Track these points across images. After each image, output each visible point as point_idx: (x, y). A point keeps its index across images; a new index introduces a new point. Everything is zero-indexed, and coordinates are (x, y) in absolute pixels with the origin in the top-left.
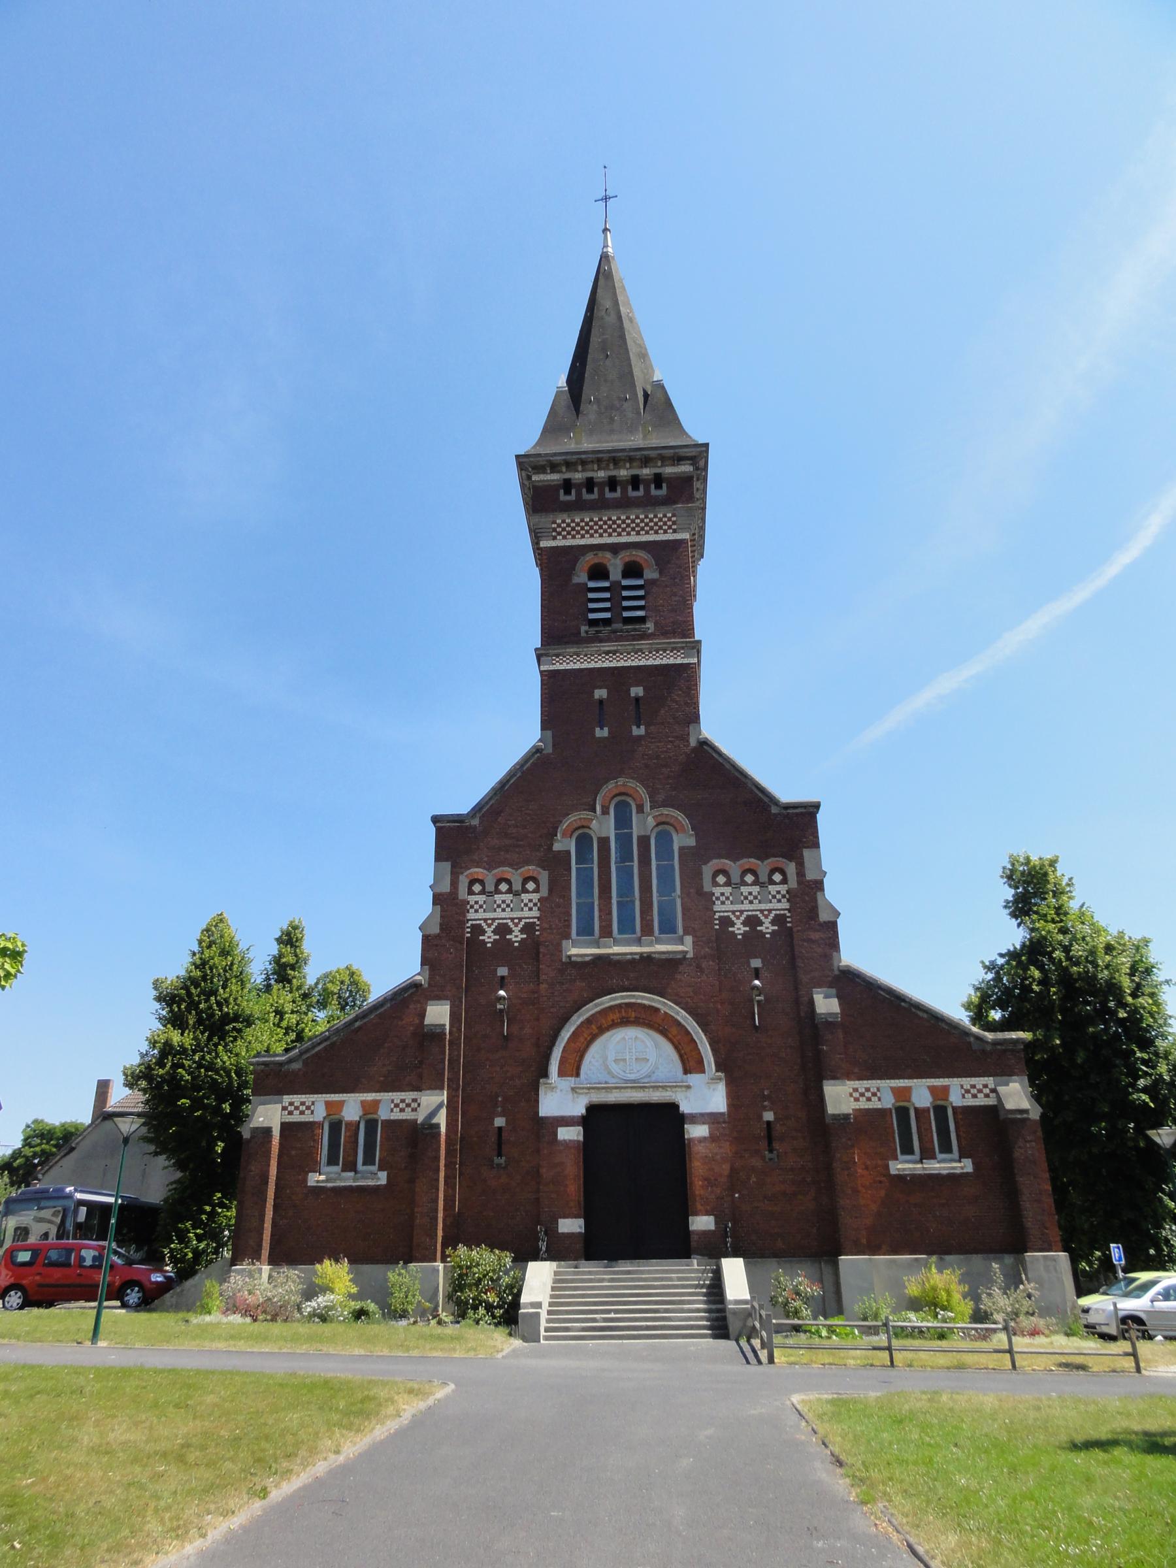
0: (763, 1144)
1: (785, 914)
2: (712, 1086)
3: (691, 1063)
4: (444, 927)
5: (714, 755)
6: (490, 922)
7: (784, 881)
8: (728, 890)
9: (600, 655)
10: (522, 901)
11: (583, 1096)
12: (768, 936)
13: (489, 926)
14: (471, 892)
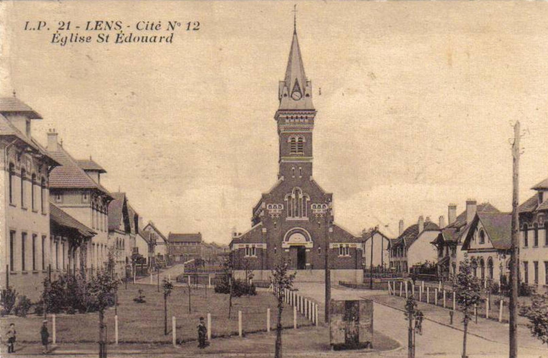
3: (307, 240)
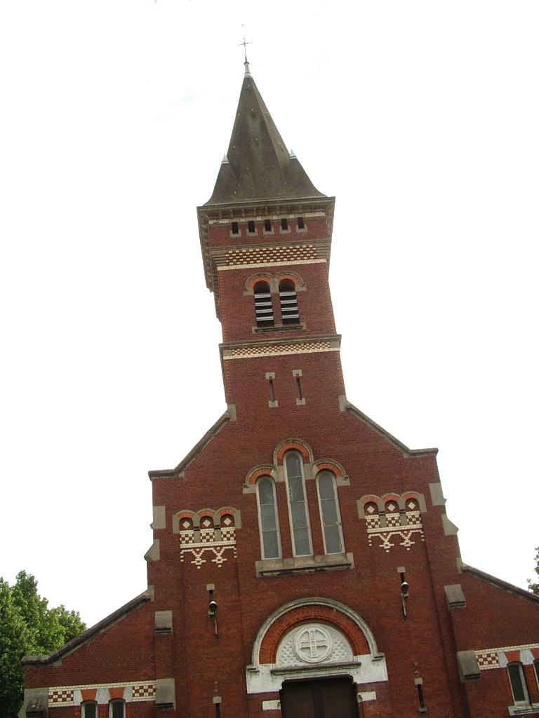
0: (417, 702)
1: (419, 532)
2: (376, 663)
3: (359, 647)
4: (163, 554)
5: (358, 417)
6: (198, 550)
7: (417, 508)
8: (376, 517)
9: (267, 347)
10: (222, 533)
11: (280, 677)
12: (408, 549)
13: (198, 553)
14: (182, 528)
